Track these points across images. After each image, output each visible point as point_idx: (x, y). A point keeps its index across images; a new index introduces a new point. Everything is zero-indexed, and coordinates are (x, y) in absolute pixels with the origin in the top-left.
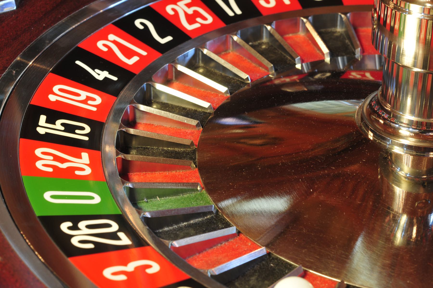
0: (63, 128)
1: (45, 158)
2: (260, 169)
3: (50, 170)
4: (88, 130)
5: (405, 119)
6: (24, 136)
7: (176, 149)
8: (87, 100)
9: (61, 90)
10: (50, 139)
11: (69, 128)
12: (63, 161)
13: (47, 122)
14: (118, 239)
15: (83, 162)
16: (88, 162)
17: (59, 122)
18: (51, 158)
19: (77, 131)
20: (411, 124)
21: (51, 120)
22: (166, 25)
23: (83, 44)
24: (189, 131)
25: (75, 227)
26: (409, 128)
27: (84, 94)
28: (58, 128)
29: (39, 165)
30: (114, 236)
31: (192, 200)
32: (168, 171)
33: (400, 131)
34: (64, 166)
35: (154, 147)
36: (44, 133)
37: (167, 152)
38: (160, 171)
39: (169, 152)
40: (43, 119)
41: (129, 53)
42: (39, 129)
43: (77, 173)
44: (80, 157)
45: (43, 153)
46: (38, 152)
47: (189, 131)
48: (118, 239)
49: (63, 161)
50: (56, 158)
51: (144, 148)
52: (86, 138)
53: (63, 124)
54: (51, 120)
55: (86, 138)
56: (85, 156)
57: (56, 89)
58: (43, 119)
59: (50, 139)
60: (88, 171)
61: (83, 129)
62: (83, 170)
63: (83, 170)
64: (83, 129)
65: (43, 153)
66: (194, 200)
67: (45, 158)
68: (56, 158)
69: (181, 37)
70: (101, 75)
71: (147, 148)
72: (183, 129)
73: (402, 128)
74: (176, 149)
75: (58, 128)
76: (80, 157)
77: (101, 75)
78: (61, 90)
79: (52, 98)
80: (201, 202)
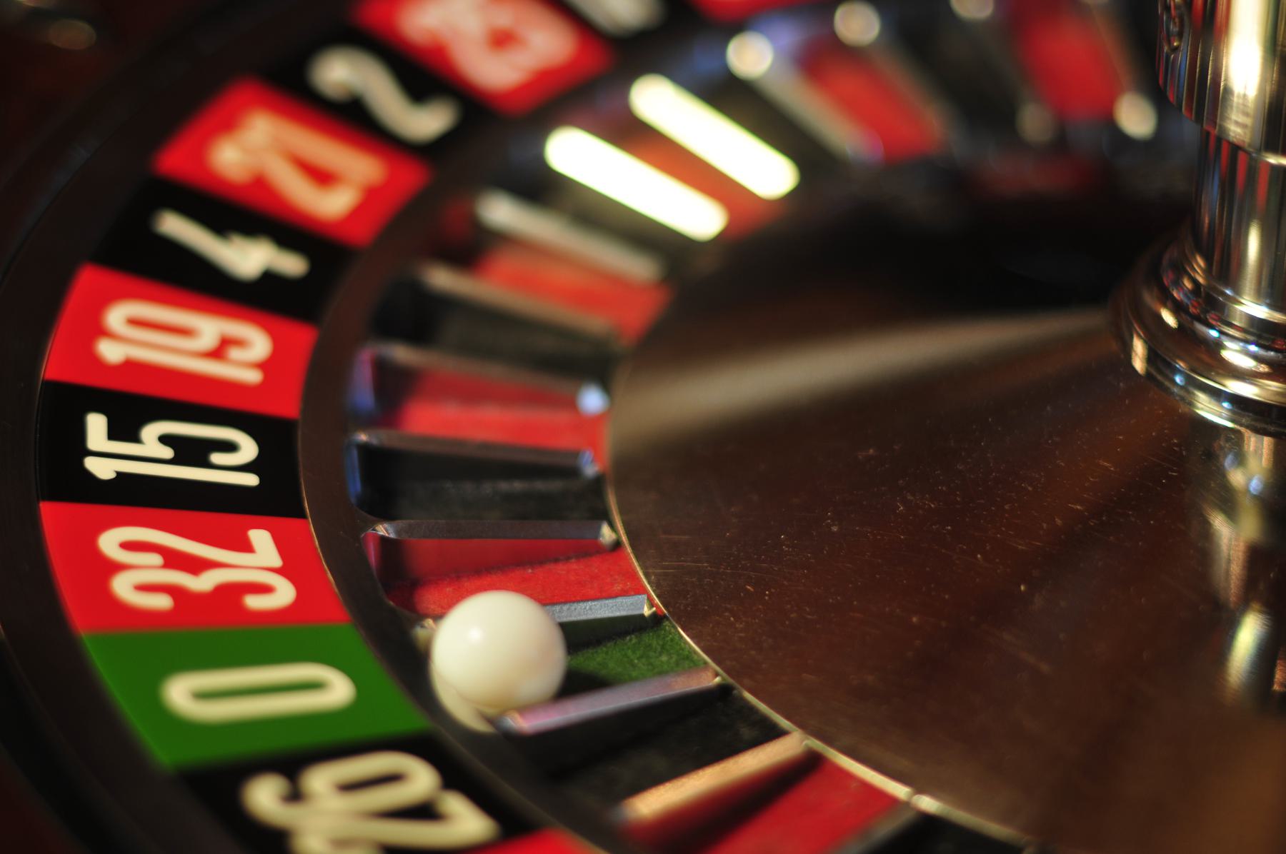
0: (168, 453)
1: (138, 565)
2: (835, 529)
3: (162, 602)
4: (248, 449)
5: (1238, 317)
6: (56, 494)
7: (540, 485)
8: (239, 351)
9: (135, 322)
10: (136, 496)
12: (196, 565)
13: (113, 435)
15: (257, 564)
16: (277, 562)
17: (152, 432)
18: (156, 559)
19: (217, 458)
20: (1260, 332)
21: (124, 429)
22: (423, 73)
23: (172, 161)
25: (295, 796)
26: (1247, 342)
27: (209, 328)
28: (150, 451)
29: (122, 586)
30: (424, 812)
31: (630, 653)
33: (1225, 354)
34: (204, 583)
36: (113, 475)
37: (509, 498)
40: (96, 425)
41: (322, 177)
42: (91, 464)
43: (254, 602)
44: (247, 547)
45: (128, 546)
46: (110, 542)
49: (196, 565)
50: (173, 560)
52: (251, 480)
53: (165, 439)
54: (124, 429)
55: (251, 480)
56: (261, 538)
57: (117, 316)
58: (96, 425)
59: (136, 496)
60: (284, 594)
61: (230, 447)
62: (264, 589)
63: (264, 589)
64: (230, 447)
65: (128, 546)
66: (638, 653)
67: (138, 565)
68: (173, 560)
69: (476, 107)
70: (248, 258)
73: (1228, 343)
75: (150, 451)
76: (247, 547)
77: (248, 258)
78: (135, 322)
79: (110, 352)
80: (664, 658)
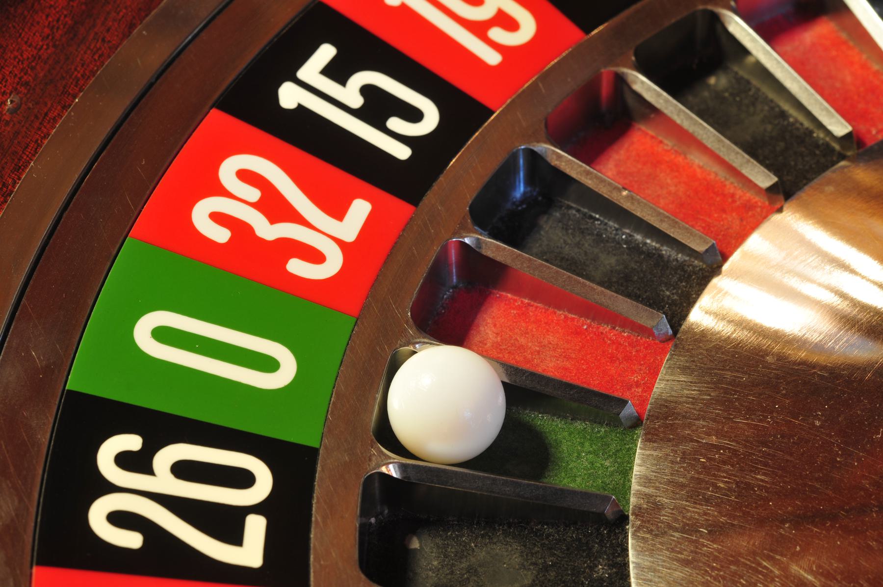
0: (357, 102)
7: (666, 250)
11: (377, 108)
13: (329, 71)
14: (235, 537)
19: (395, 124)
24: (750, 195)
30: (226, 524)
32: (593, 320)
35: (611, 223)
38: (570, 311)
39: (642, 252)
44: (338, 212)
47: (750, 195)
48: (235, 537)
51: (585, 214)
53: (368, 91)
62: (316, 257)
63: (316, 257)
71: (591, 217)
72: (731, 185)
74: (666, 250)
76: (338, 212)
